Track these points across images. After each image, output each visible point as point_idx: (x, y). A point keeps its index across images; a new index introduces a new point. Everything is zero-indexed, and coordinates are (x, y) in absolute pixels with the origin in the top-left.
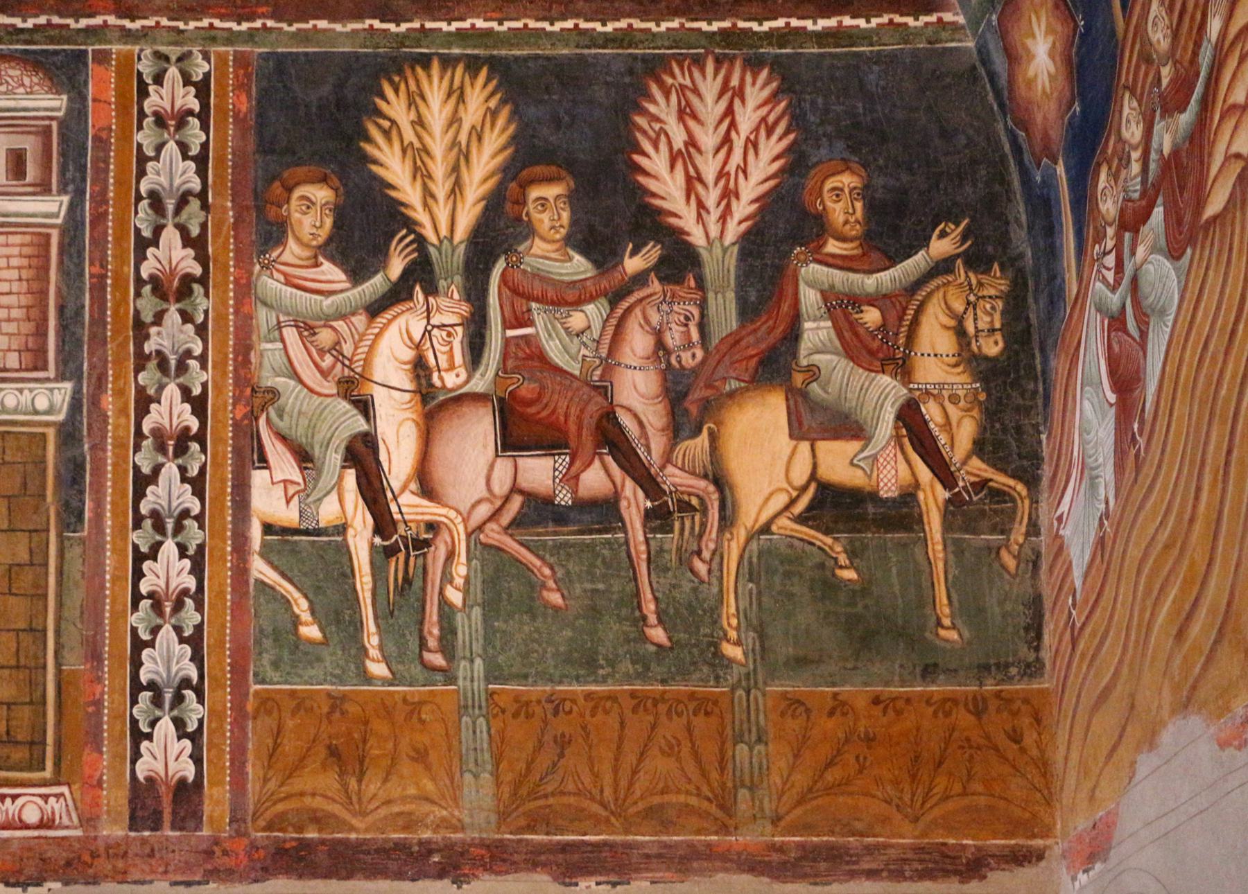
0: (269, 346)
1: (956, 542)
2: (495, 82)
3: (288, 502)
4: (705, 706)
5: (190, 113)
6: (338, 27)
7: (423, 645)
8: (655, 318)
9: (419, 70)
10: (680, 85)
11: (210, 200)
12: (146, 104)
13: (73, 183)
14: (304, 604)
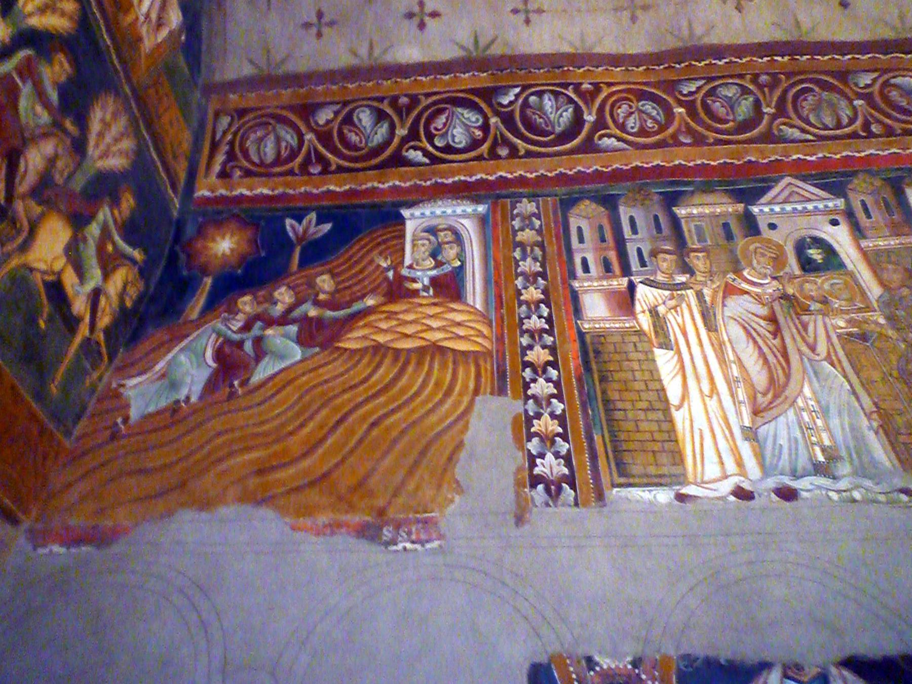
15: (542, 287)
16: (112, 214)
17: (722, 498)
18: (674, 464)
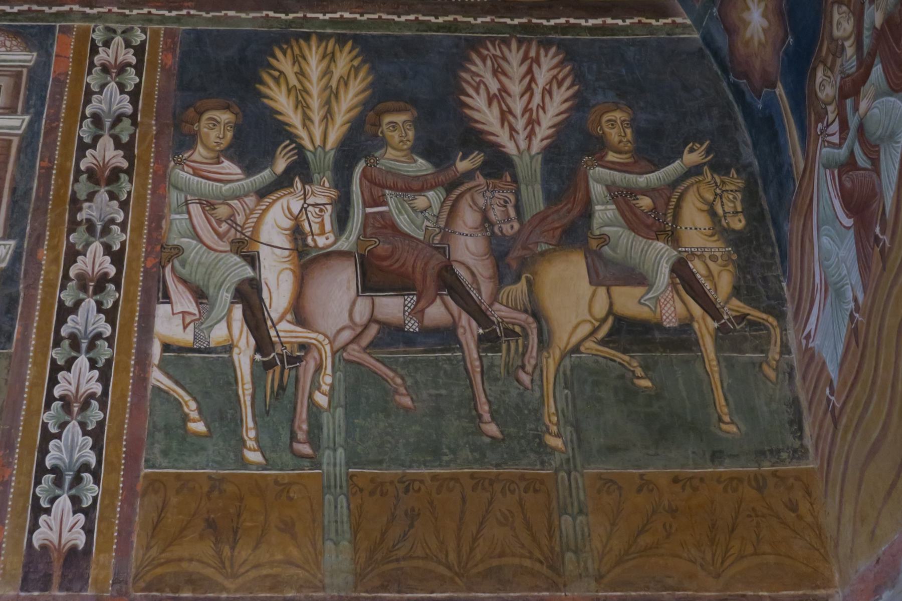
0: (178, 216)
1: (727, 359)
2: (357, 50)
3: (185, 328)
4: (534, 485)
5: (129, 65)
6: (243, 15)
7: (293, 437)
8: (481, 201)
9: (302, 42)
10: (493, 55)
11: (139, 119)
12: (96, 59)
13: (34, 107)
14: (193, 405)
16: (612, 166)
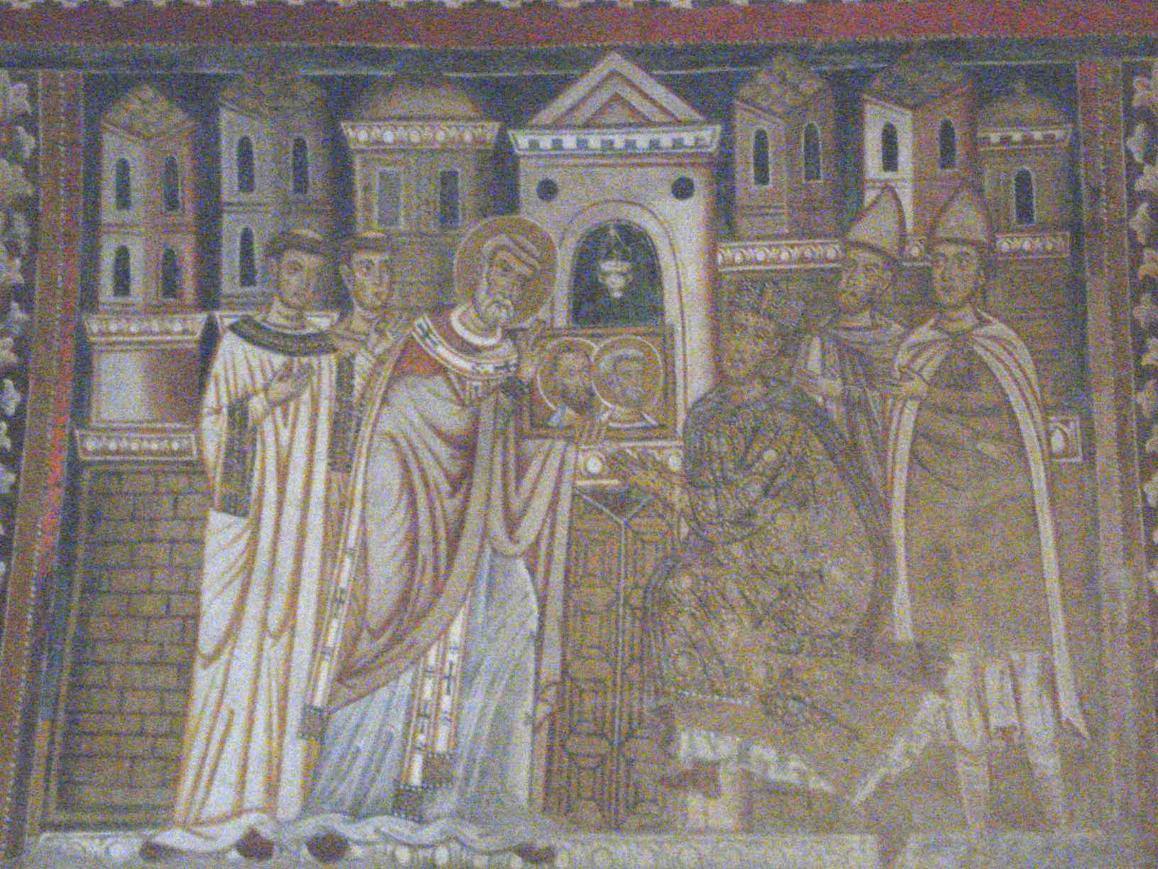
15: (16, 330)
17: (219, 855)
18: (164, 784)
